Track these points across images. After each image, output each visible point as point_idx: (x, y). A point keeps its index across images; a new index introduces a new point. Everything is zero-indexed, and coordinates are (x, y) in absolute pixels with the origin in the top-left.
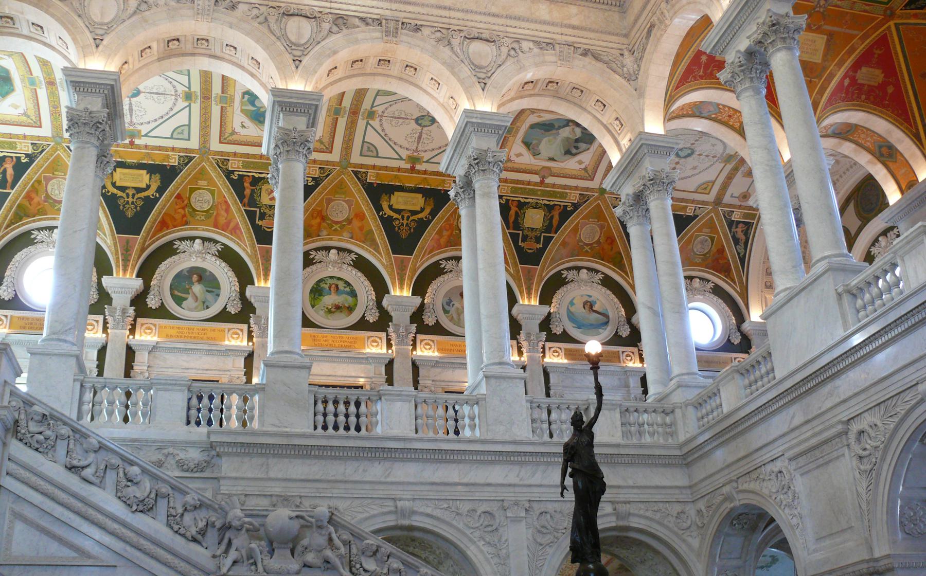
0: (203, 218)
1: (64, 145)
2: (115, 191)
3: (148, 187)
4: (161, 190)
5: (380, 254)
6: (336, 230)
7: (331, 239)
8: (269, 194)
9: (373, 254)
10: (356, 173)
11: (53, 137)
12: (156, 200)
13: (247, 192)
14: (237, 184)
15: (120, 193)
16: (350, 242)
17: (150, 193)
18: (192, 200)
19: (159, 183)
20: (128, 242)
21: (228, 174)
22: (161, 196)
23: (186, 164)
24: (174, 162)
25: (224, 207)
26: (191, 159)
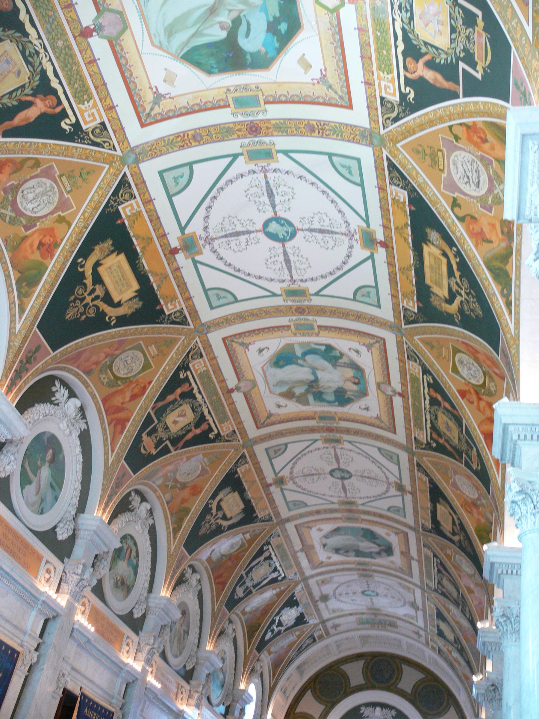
0: (106, 381)
1: (126, 169)
2: (89, 273)
3: (119, 305)
4: (122, 321)
5: (175, 538)
6: (167, 486)
7: (155, 491)
8: (179, 416)
9: (168, 533)
10: (243, 457)
11: (133, 150)
12: (108, 326)
13: (170, 398)
14: (175, 382)
15: (89, 281)
16: (162, 504)
17: (112, 313)
18: (123, 356)
19: (130, 312)
20: (38, 348)
21: (184, 367)
22: (115, 326)
23: (173, 323)
24: (169, 309)
25: (136, 391)
26: (184, 322)
